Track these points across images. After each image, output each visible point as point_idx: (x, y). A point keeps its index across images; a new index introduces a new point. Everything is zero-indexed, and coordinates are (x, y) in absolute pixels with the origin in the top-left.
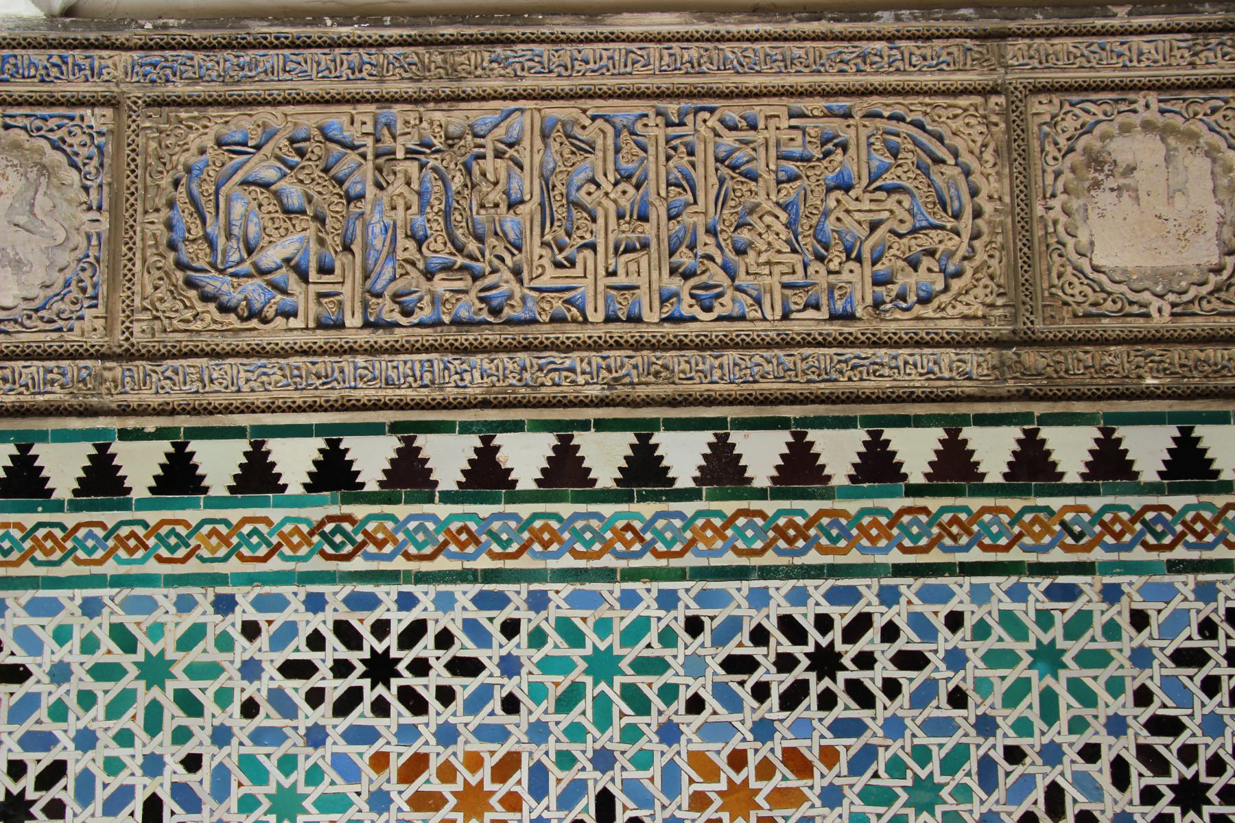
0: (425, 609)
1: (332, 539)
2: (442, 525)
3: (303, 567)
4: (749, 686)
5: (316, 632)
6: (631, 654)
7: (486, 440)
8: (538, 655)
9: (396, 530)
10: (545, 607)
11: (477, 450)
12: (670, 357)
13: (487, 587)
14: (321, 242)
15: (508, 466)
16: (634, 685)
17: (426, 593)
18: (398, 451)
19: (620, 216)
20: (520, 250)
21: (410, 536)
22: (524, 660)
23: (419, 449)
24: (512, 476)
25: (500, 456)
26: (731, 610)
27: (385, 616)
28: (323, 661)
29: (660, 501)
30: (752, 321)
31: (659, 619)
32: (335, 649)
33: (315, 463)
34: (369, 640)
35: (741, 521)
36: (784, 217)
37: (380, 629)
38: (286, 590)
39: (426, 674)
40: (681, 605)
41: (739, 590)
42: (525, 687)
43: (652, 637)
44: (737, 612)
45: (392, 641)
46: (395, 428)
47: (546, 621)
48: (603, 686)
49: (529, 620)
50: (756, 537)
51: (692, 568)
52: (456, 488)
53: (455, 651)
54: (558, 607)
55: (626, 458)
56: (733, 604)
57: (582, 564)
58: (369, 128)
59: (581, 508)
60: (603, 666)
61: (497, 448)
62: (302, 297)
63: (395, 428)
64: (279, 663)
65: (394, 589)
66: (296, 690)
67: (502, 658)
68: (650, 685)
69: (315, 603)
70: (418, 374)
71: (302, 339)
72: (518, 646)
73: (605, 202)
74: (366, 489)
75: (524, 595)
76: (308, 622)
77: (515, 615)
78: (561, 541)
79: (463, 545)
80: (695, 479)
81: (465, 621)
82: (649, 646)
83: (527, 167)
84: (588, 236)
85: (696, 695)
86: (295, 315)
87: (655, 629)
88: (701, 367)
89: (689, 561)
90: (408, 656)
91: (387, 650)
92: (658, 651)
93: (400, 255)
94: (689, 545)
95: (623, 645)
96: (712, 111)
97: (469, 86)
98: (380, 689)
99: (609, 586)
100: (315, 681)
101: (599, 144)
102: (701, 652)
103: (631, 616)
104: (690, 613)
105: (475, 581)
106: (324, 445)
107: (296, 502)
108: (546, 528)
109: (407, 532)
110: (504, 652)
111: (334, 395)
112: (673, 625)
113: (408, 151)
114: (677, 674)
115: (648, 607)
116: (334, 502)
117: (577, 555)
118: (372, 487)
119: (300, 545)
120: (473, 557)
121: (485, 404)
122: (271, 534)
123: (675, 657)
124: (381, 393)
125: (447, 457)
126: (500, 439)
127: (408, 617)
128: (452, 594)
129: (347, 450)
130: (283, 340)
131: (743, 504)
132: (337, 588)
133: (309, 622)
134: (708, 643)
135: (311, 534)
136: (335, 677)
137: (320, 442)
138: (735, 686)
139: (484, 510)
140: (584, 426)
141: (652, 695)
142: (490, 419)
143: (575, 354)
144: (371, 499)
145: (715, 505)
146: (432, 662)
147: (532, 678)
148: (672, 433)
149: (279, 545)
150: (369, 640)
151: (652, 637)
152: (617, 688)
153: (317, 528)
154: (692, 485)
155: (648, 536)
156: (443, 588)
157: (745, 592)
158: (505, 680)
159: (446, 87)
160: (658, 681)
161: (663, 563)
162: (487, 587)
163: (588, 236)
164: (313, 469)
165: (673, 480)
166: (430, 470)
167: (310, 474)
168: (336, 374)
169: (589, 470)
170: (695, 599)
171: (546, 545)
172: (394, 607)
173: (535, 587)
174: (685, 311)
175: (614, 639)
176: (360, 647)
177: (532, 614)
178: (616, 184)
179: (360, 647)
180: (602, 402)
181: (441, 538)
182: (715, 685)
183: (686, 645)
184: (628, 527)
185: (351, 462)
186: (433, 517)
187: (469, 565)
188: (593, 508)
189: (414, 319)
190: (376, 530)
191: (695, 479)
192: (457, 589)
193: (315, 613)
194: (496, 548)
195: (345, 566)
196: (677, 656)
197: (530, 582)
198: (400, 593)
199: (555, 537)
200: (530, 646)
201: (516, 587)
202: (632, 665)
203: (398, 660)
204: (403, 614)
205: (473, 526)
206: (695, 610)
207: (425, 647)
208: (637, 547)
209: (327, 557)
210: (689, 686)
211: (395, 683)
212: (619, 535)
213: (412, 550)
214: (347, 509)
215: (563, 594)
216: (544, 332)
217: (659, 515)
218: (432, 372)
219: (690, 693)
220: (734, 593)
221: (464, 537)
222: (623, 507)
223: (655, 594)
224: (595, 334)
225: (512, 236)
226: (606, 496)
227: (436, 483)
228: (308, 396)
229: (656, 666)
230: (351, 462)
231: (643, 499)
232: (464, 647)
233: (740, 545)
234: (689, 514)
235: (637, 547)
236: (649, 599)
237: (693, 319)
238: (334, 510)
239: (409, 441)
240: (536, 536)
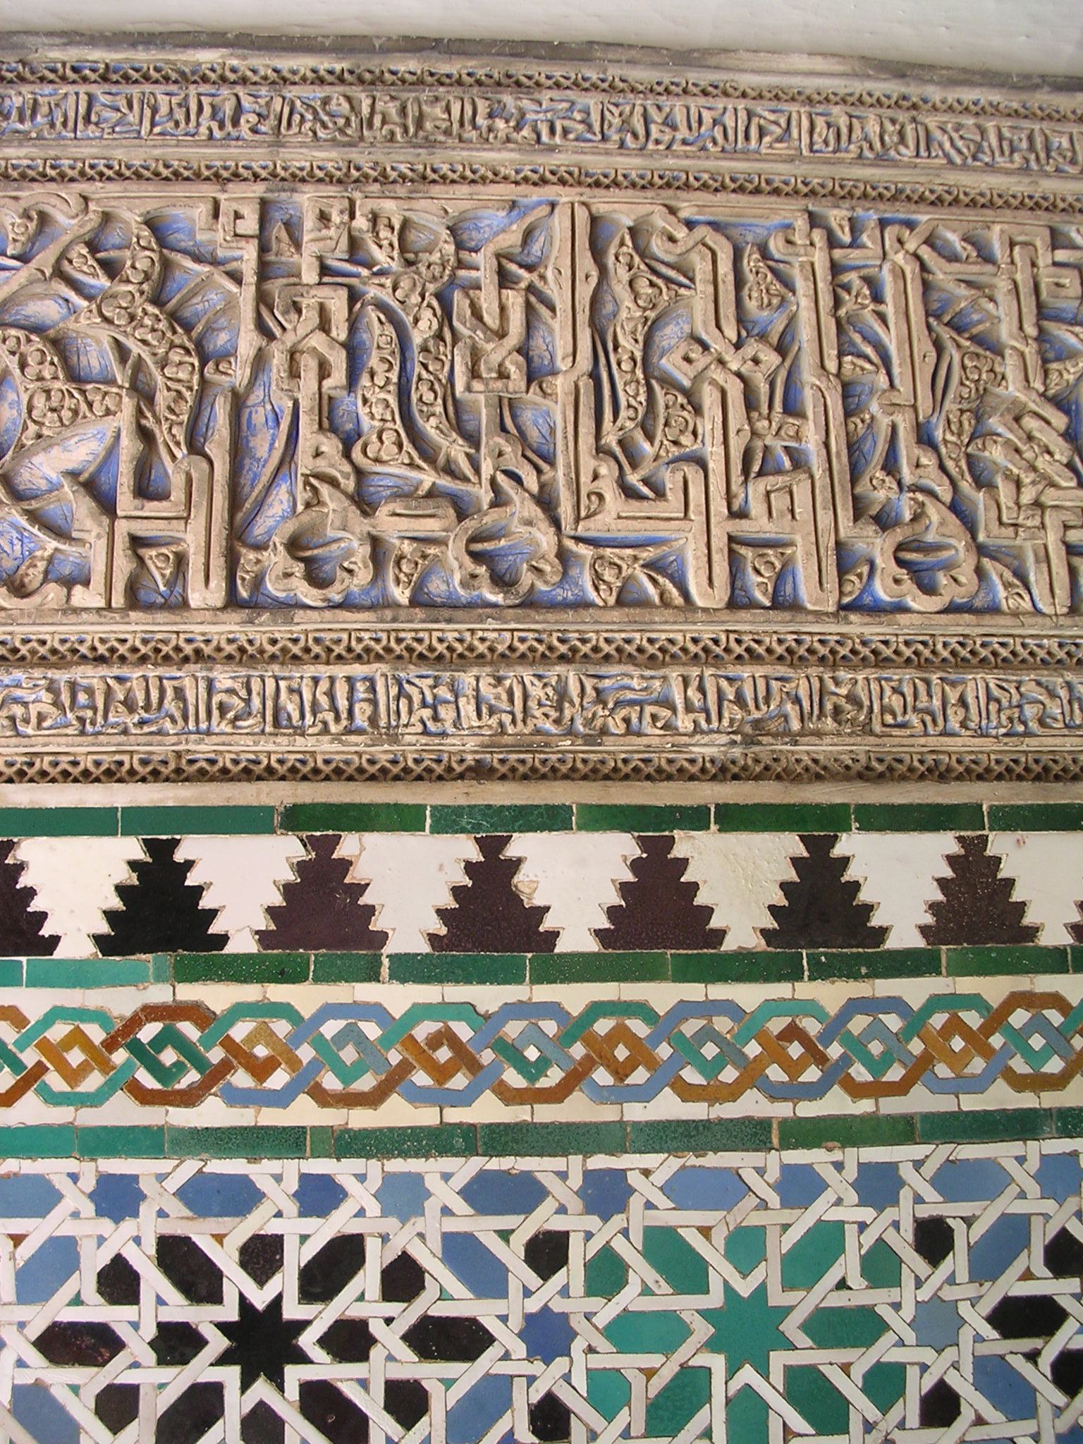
0: (361, 1213)
1: (157, 1056)
2: (398, 1030)
3: (89, 1117)
4: (1046, 1360)
5: (119, 1261)
6: (805, 1303)
7: (492, 846)
8: (607, 1312)
9: (296, 1039)
10: (622, 1207)
11: (470, 868)
12: (860, 680)
13: (495, 1164)
14: (145, 435)
15: (538, 901)
16: (813, 1369)
17: (362, 1178)
18: (301, 867)
19: (750, 403)
20: (552, 463)
21: (327, 1053)
22: (577, 1323)
23: (346, 864)
24: (548, 924)
25: (521, 879)
26: (1007, 1204)
27: (274, 1227)
28: (135, 1324)
29: (856, 976)
30: (1016, 614)
31: (863, 1227)
32: (161, 1300)
33: (121, 890)
34: (237, 1281)
35: (1019, 1018)
36: (1060, 421)
37: (262, 1256)
38: (54, 1168)
39: (363, 1357)
40: (905, 1195)
41: (1021, 1160)
42: (580, 1380)
43: (849, 1265)
44: (1019, 1207)
45: (286, 1282)
46: (294, 819)
47: (623, 1235)
48: (748, 1375)
49: (587, 1235)
50: (1050, 1050)
51: (928, 1117)
52: (426, 948)
53: (426, 1304)
54: (649, 1205)
55: (784, 886)
56: (1013, 1190)
57: (697, 1111)
58: (250, 225)
59: (694, 992)
60: (747, 1329)
61: (516, 864)
62: (102, 544)
63: (294, 819)
64: (35, 1331)
65: (292, 1169)
66: (75, 1389)
67: (529, 1318)
68: (846, 1368)
69: (117, 1199)
70: (342, 704)
71: (94, 631)
72: (565, 1292)
73: (717, 374)
74: (229, 949)
75: (576, 1181)
76: (101, 1240)
77: (558, 1224)
78: (652, 1063)
79: (442, 1073)
80: (924, 930)
81: (448, 1238)
82: (842, 1285)
83: (562, 304)
84: (686, 440)
85: (941, 1386)
86: (86, 583)
87: (854, 1248)
88: (923, 702)
89: (920, 1101)
90: (323, 1317)
91: (277, 1303)
92: (861, 1295)
93: (304, 462)
94: (919, 1070)
95: (788, 1286)
96: (910, 225)
97: (442, 160)
98: (262, 1390)
99: (756, 1158)
100: (116, 1372)
101: (702, 268)
102: (948, 1294)
103: (803, 1222)
104: (924, 1212)
105: (469, 1150)
106: (139, 854)
107: (77, 975)
108: (621, 1034)
109: (320, 1043)
110: (533, 1305)
111: (161, 750)
112: (891, 1238)
113: (325, 270)
114: (901, 1343)
115: (839, 1204)
116: (159, 979)
117: (687, 1093)
118: (242, 944)
119: (84, 1070)
120: (465, 1098)
121: (480, 772)
122: (22, 1044)
123: (897, 1306)
124: (266, 745)
125: (409, 881)
126: (521, 845)
127: (323, 1231)
128: (418, 1178)
129: (189, 865)
130: (54, 633)
131: (1022, 983)
132: (164, 1165)
133: (103, 1241)
134: (963, 1276)
135: (111, 1044)
136: (161, 1362)
137: (132, 848)
138: (1019, 1363)
139: (489, 997)
140: (695, 818)
141: (850, 1388)
142: (497, 801)
143: (674, 674)
144: (241, 970)
145: (967, 985)
146: (376, 1328)
147: (596, 1362)
148: (874, 837)
149: (40, 1069)
150: (237, 1281)
151: (849, 1265)
152: (777, 1377)
153: (122, 1035)
154: (919, 942)
155: (835, 1051)
156: (397, 1165)
157: (1034, 1164)
158: (537, 1367)
159: (401, 160)
160: (863, 1360)
161: (865, 1106)
162: (495, 1164)
163: (686, 440)
164: (116, 903)
165: (882, 932)
166: (371, 910)
167: (110, 915)
168: (170, 705)
169: (708, 911)
170: (935, 1182)
171: (620, 1072)
172: (291, 1208)
173: (599, 1162)
174: (882, 591)
175: (768, 1272)
176: (215, 1297)
177: (593, 1222)
178: (738, 346)
179: (215, 1297)
180: (723, 772)
181: (394, 1057)
182: (980, 1363)
183: (920, 1283)
184: (793, 1033)
185: (198, 891)
186: (376, 1012)
187: (455, 1115)
188: (719, 991)
189: (335, 594)
190: (252, 1039)
191: (924, 930)
192: (430, 1168)
193: (117, 1220)
194: (514, 1079)
195: (181, 1117)
196: (900, 1305)
197: (587, 1154)
198: (304, 1178)
199: (641, 1054)
200: (590, 1292)
201: (558, 1163)
202: (806, 1327)
203: (302, 1325)
204: (310, 1224)
205: (463, 1031)
206: (935, 1206)
207: (361, 1296)
208: (812, 1074)
209: (144, 1097)
210: (927, 1368)
211: (294, 1375)
212: (774, 1050)
213: (331, 1082)
214: (189, 992)
215: (660, 1177)
216: (606, 628)
217: (854, 1006)
218: (374, 702)
219: (929, 1382)
220: (1012, 1167)
221: (444, 1054)
222: (781, 990)
223: (851, 1172)
224: (707, 632)
225: (534, 435)
226: (746, 967)
227: (383, 937)
228: (106, 749)
229: (857, 1327)
230: (198, 891)
231: (821, 972)
232: (448, 1295)
233: (1019, 1065)
234: (916, 1004)
235: (812, 1074)
236: (840, 1185)
237: (902, 609)
238: (160, 994)
239: (324, 847)
240: (600, 1053)
